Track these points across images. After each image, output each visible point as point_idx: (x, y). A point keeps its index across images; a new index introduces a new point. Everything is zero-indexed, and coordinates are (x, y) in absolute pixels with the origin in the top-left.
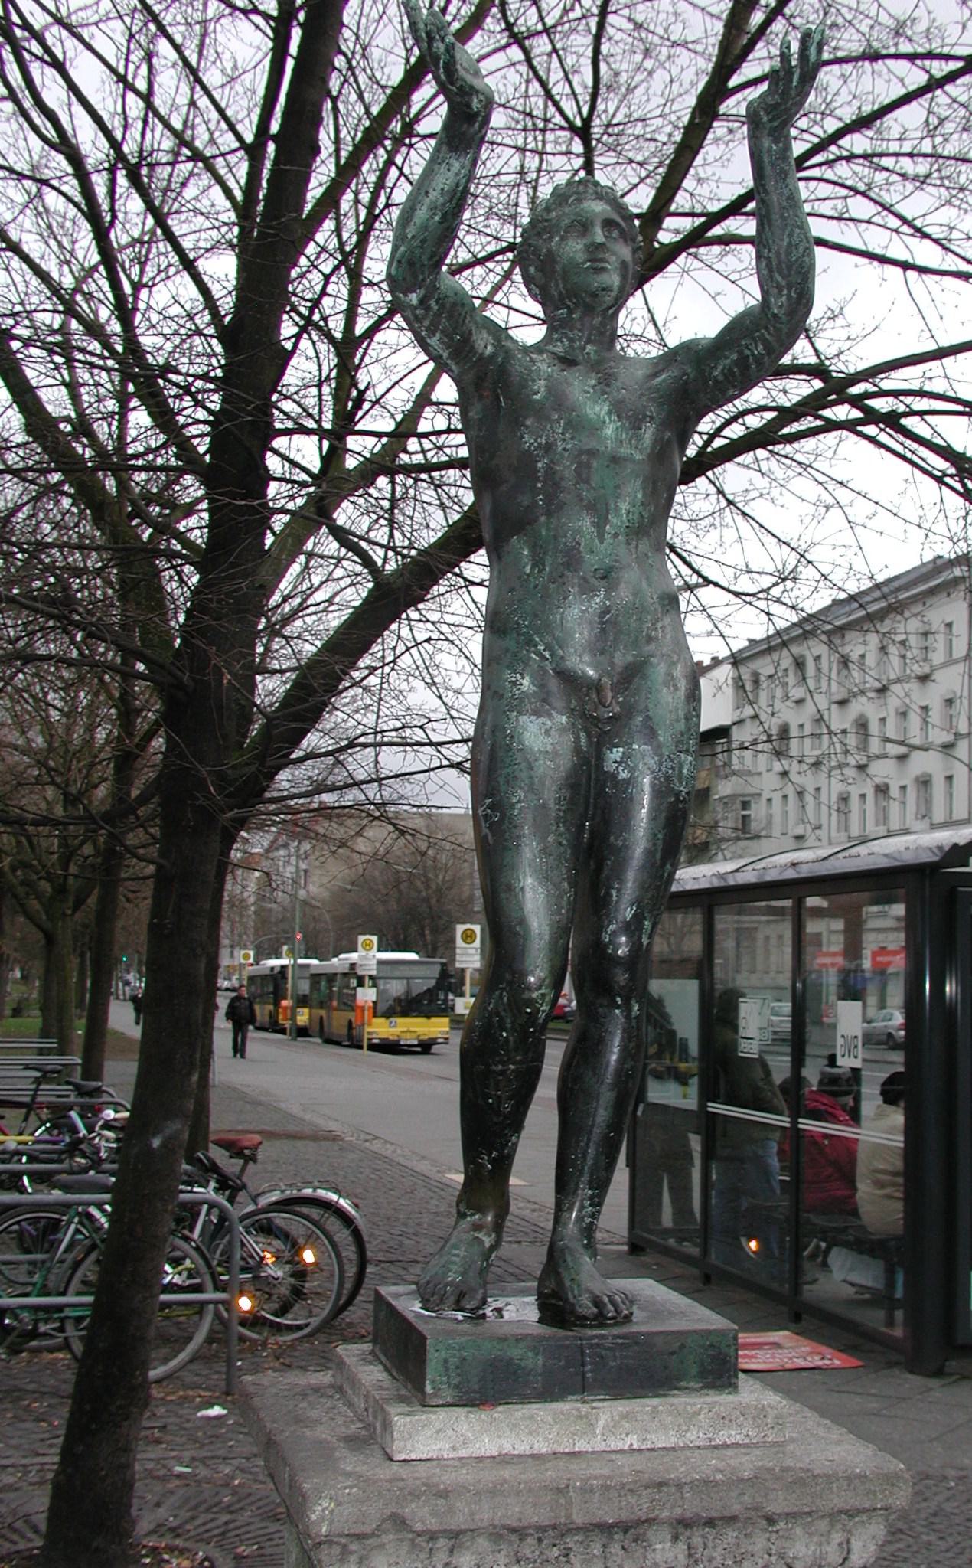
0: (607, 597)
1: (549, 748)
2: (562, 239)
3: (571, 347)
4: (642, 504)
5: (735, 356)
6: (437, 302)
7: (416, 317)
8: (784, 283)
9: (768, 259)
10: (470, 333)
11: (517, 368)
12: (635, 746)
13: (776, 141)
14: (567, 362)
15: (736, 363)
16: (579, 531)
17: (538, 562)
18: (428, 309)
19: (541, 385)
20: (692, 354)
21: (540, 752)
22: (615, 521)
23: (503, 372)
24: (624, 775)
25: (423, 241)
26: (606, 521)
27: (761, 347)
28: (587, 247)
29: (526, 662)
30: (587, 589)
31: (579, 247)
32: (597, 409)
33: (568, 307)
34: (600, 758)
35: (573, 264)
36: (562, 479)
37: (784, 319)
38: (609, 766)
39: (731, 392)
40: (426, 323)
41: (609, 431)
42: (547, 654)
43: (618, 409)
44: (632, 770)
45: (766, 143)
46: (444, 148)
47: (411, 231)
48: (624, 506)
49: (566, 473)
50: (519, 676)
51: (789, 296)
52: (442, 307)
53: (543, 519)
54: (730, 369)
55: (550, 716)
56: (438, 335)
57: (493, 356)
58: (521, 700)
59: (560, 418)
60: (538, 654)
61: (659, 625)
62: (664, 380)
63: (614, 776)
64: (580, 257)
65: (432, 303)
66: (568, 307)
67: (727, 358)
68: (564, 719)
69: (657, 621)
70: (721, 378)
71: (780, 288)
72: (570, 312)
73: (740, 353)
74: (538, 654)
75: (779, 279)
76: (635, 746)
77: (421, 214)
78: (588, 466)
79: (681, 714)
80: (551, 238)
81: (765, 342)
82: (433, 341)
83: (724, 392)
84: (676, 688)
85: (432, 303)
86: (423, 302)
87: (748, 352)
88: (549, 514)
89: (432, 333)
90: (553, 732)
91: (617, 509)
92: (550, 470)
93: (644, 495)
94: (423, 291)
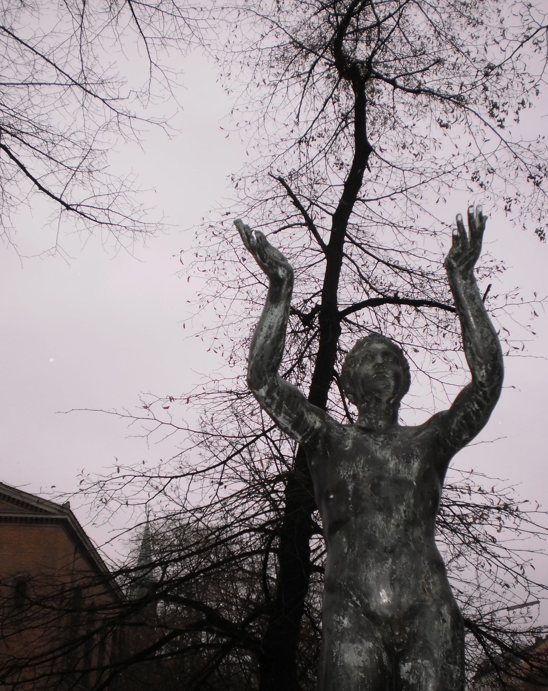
0: (393, 563)
1: (362, 664)
2: (361, 365)
3: (370, 423)
4: (414, 506)
5: (462, 414)
6: (278, 394)
7: (267, 404)
8: (482, 362)
9: (470, 348)
10: (303, 414)
11: (335, 434)
12: (419, 661)
13: (465, 278)
14: (367, 430)
15: (464, 417)
16: (375, 524)
17: (351, 545)
18: (273, 398)
19: (349, 443)
20: (439, 420)
21: (355, 667)
22: (397, 517)
23: (327, 438)
24: (412, 681)
25: (262, 357)
26: (391, 517)
27: (476, 406)
28: (374, 367)
29: (346, 608)
30: (381, 560)
31: (369, 368)
32: (384, 453)
33: (367, 401)
34: (397, 669)
35: (367, 376)
36: (363, 494)
37: (486, 384)
38: (404, 675)
39: (464, 437)
40: (274, 407)
41: (392, 465)
42: (358, 603)
43: (396, 452)
44: (418, 678)
45: (460, 281)
46: (269, 302)
47: (255, 353)
48: (402, 508)
49: (365, 491)
50: (341, 618)
51: (487, 370)
52: (282, 397)
53: (353, 519)
54: (461, 423)
55: (361, 643)
56: (283, 415)
57: (320, 429)
58: (343, 633)
59: (361, 459)
60: (354, 603)
61: (431, 581)
62: (424, 435)
63: (406, 682)
64: (371, 373)
65: (275, 395)
66: (367, 401)
67: (458, 415)
68: (371, 645)
69: (429, 578)
70: (457, 429)
71: (480, 365)
72: (368, 404)
73: (465, 411)
74: (354, 603)
75: (479, 359)
76: (419, 661)
77: (261, 340)
78: (378, 485)
79: (449, 637)
80: (355, 365)
81: (479, 404)
82: (280, 419)
83: (460, 437)
84: (444, 621)
85: (275, 395)
86: (268, 393)
87: (469, 410)
88: (356, 516)
89: (278, 413)
90: (363, 654)
91: (398, 510)
92: (356, 489)
93: (415, 501)
94: (266, 387)
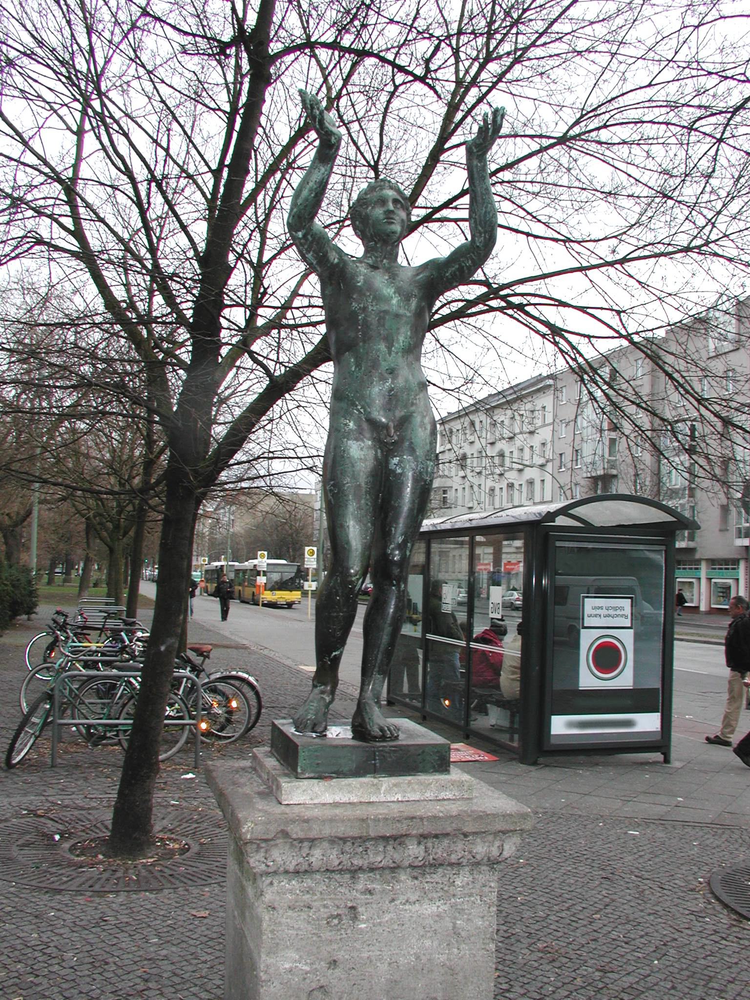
0: (392, 383)
1: (363, 457)
2: (373, 208)
5: (457, 266)
10: (327, 252)
13: (480, 162)
14: (374, 267)
16: (379, 350)
17: (358, 365)
18: (307, 240)
25: (306, 206)
26: (393, 346)
28: (385, 212)
29: (352, 414)
30: (383, 379)
34: (387, 462)
35: (377, 220)
36: (371, 324)
38: (392, 466)
41: (394, 302)
42: (362, 410)
43: (399, 291)
44: (403, 468)
45: (475, 162)
46: (317, 161)
47: (299, 201)
48: (401, 339)
49: (373, 321)
51: (485, 237)
52: (314, 239)
53: (361, 344)
55: (364, 442)
57: (338, 264)
58: (349, 433)
60: (358, 410)
63: (394, 471)
65: (309, 237)
71: (480, 233)
72: (376, 243)
73: (460, 265)
77: (305, 193)
78: (384, 318)
79: (428, 441)
80: (367, 208)
81: (472, 259)
82: (309, 256)
83: (451, 283)
84: (426, 429)
85: (309, 237)
86: (305, 236)
88: (364, 342)
92: (364, 319)
94: (304, 231)
